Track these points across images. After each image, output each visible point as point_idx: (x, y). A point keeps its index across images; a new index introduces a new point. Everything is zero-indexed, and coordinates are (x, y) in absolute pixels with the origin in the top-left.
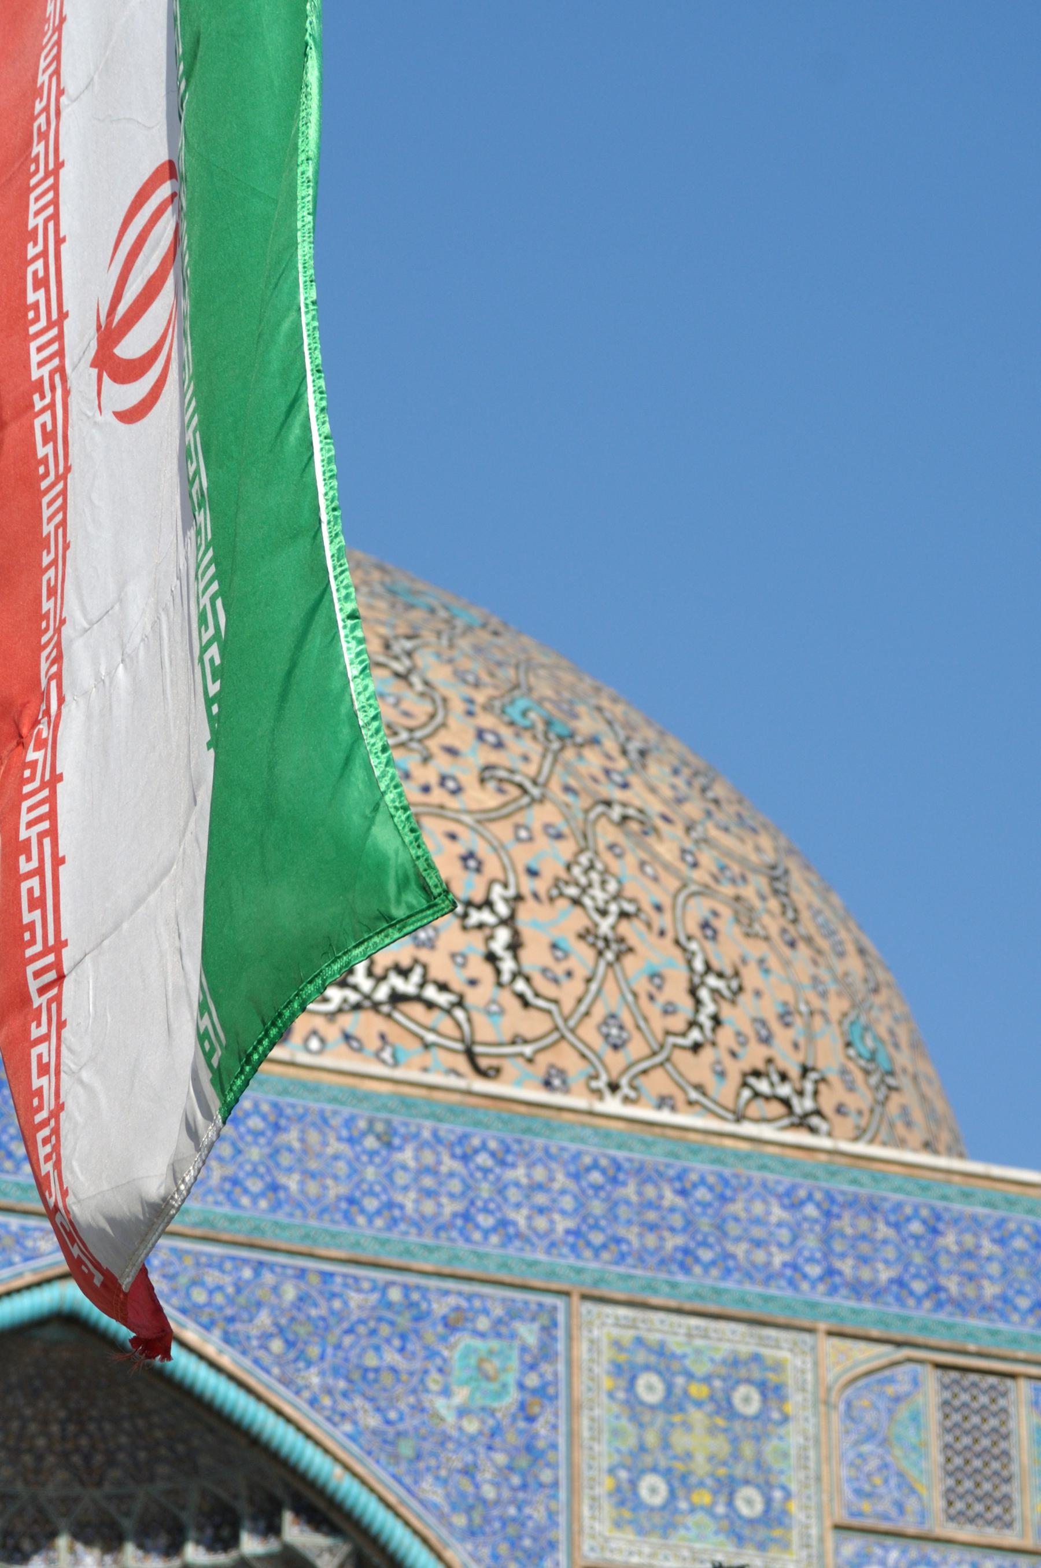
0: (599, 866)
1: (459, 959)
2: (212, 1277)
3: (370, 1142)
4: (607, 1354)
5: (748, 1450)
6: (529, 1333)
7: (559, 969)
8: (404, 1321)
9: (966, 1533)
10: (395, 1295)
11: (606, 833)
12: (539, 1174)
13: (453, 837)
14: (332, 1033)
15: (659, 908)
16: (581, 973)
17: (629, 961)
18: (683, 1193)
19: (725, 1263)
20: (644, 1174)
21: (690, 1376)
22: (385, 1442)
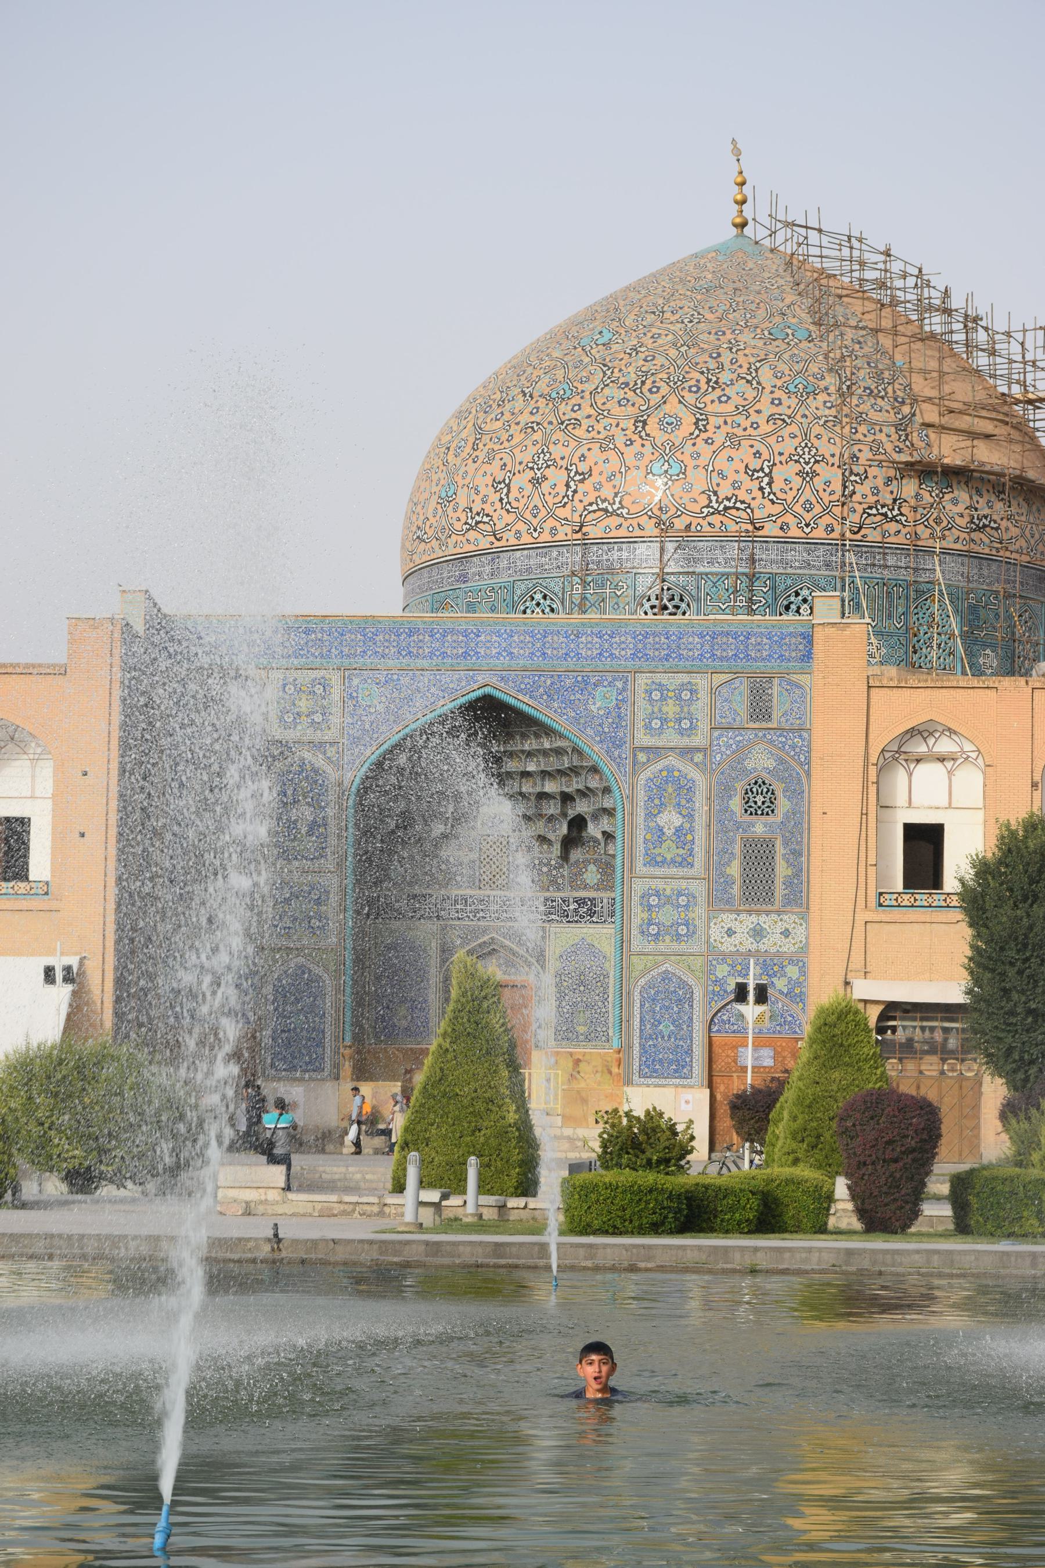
0: (809, 445)
1: (749, 491)
2: (527, 680)
3: (572, 637)
4: (644, 687)
5: (686, 709)
6: (619, 684)
7: (787, 488)
9: (757, 725)
10: (580, 678)
11: (817, 430)
12: (623, 639)
13: (752, 446)
14: (704, 523)
16: (795, 487)
18: (667, 638)
19: (680, 657)
20: (655, 635)
21: (668, 690)
22: (576, 720)
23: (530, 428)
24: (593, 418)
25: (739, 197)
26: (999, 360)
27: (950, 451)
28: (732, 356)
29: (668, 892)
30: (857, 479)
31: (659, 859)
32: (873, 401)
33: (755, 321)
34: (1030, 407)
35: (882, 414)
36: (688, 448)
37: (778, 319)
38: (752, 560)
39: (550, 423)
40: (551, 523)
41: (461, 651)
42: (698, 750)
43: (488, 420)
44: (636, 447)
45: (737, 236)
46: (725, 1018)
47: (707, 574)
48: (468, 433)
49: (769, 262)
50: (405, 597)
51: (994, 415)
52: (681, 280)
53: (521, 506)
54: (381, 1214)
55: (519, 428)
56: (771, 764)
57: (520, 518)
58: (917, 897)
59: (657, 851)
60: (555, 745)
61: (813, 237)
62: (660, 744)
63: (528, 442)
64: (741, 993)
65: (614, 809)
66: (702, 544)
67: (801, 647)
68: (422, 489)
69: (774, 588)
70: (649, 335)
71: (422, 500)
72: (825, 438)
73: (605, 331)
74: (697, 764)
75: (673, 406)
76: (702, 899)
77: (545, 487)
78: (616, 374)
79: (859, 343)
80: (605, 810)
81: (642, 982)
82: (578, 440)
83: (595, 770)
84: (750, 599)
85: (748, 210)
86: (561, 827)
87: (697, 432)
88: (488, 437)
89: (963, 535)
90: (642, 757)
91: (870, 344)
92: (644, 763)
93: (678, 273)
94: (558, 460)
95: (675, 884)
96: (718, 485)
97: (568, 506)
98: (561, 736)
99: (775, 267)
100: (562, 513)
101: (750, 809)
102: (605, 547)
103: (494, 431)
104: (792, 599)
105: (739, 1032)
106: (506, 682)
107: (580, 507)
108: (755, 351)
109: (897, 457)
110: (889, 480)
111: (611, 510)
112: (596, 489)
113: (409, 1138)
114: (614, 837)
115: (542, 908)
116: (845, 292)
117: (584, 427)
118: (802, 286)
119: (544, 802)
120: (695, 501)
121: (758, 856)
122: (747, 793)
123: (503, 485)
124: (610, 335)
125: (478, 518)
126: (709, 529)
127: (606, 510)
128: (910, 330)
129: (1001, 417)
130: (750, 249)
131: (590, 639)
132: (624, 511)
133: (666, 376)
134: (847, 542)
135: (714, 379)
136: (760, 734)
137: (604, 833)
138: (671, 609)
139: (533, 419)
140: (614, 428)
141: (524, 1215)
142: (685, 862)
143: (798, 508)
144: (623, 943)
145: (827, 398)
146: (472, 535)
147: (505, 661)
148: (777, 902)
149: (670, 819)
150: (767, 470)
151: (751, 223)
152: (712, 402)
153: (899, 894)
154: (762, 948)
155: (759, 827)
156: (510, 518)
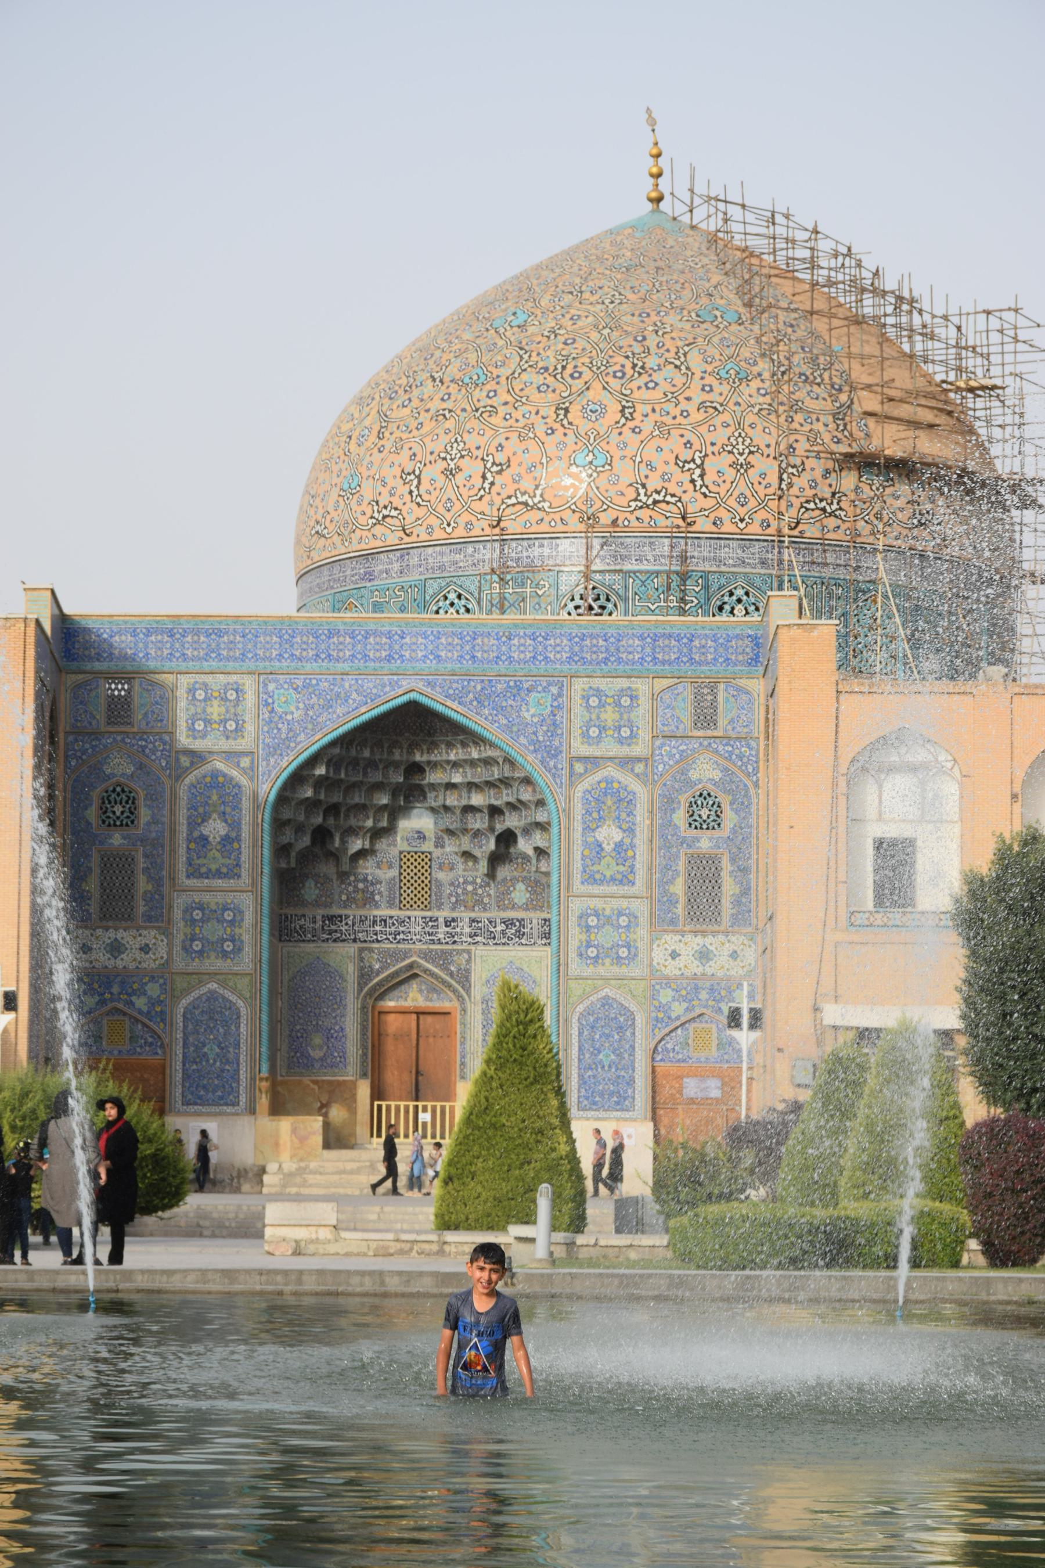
1: (680, 484)
2: (455, 685)
3: (504, 639)
4: (580, 693)
5: (625, 717)
6: (554, 690)
7: (720, 481)
8: (515, 691)
10: (512, 684)
11: (750, 418)
12: (558, 641)
13: (682, 436)
14: (632, 518)
15: (768, 446)
17: (751, 471)
19: (619, 661)
22: (508, 728)
23: (442, 415)
24: (511, 405)
25: (655, 170)
26: (937, 345)
27: (891, 442)
28: (658, 339)
29: (608, 912)
30: (794, 471)
31: (597, 876)
32: (809, 388)
33: (681, 302)
34: (970, 395)
35: (817, 402)
36: (614, 438)
37: (704, 300)
38: (684, 558)
39: (464, 410)
40: (466, 517)
41: (384, 654)
42: (639, 760)
43: (394, 407)
44: (558, 436)
45: (653, 211)
46: (670, 1046)
47: (635, 572)
48: (372, 420)
49: (690, 240)
50: (301, 595)
51: (933, 403)
52: (598, 258)
53: (433, 498)
54: (441, 1252)
55: (428, 415)
56: (717, 775)
57: (433, 511)
58: (891, 915)
59: (595, 868)
60: (484, 755)
61: (735, 212)
62: (598, 754)
63: (440, 431)
64: (734, 1019)
65: (549, 823)
66: (629, 540)
67: (748, 650)
68: (320, 480)
69: (706, 587)
70: (568, 316)
71: (321, 492)
72: (760, 428)
73: (519, 312)
74: (637, 775)
75: (596, 392)
76: (643, 920)
77: (460, 479)
78: (534, 358)
79: (792, 326)
80: (538, 825)
81: (581, 1008)
82: (495, 429)
83: (527, 781)
84: (682, 600)
85: (664, 184)
86: (488, 842)
87: (623, 420)
88: (395, 425)
89: (905, 532)
90: (579, 768)
91: (803, 327)
92: (581, 775)
93: (593, 251)
94: (473, 450)
95: (616, 904)
96: (647, 477)
97: (487, 498)
98: (492, 745)
99: (697, 245)
100: (477, 506)
101: (696, 823)
102: (525, 543)
103: (402, 419)
104: (726, 599)
105: (684, 1061)
106: (433, 688)
107: (497, 500)
108: (682, 335)
109: (835, 448)
110: (827, 472)
111: (531, 503)
112: (514, 481)
113: (453, 1171)
114: (548, 855)
115: (467, 930)
116: (773, 272)
117: (501, 414)
118: (728, 266)
119: (470, 816)
120: (622, 494)
121: (704, 875)
122: (691, 806)
123: (412, 477)
124: (525, 317)
125: (385, 512)
126: (634, 523)
127: (526, 504)
128: (841, 312)
129: (940, 405)
130: (668, 225)
131: (522, 641)
132: (546, 505)
133: (588, 360)
134: (786, 539)
135: (640, 364)
136: (706, 743)
137: (536, 849)
138: (597, 610)
139: (445, 405)
140: (533, 415)
141: (594, 1252)
142: (625, 879)
143: (732, 502)
144: (559, 967)
145: (761, 385)
146: (378, 530)
147: (431, 664)
148: (724, 923)
149: (609, 834)
150: (698, 462)
151: (668, 198)
152: (639, 388)
153: (871, 912)
154: (709, 971)
155: (705, 842)
156: (420, 512)
